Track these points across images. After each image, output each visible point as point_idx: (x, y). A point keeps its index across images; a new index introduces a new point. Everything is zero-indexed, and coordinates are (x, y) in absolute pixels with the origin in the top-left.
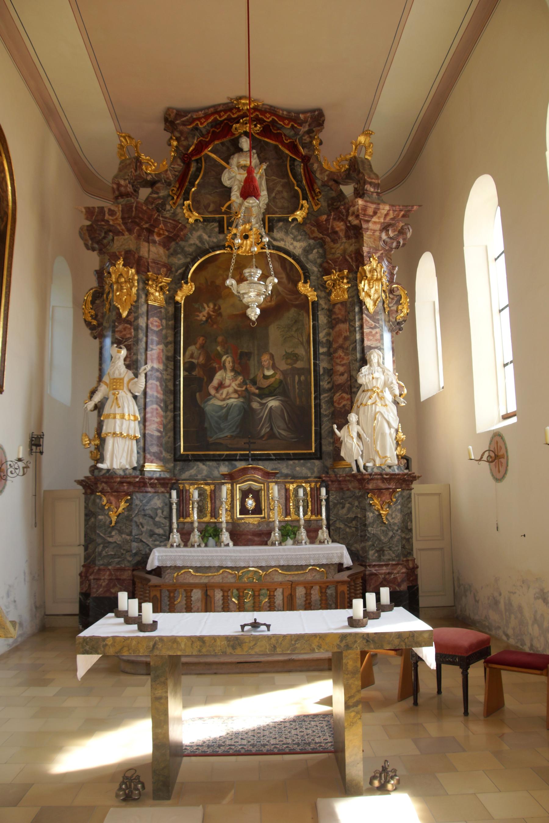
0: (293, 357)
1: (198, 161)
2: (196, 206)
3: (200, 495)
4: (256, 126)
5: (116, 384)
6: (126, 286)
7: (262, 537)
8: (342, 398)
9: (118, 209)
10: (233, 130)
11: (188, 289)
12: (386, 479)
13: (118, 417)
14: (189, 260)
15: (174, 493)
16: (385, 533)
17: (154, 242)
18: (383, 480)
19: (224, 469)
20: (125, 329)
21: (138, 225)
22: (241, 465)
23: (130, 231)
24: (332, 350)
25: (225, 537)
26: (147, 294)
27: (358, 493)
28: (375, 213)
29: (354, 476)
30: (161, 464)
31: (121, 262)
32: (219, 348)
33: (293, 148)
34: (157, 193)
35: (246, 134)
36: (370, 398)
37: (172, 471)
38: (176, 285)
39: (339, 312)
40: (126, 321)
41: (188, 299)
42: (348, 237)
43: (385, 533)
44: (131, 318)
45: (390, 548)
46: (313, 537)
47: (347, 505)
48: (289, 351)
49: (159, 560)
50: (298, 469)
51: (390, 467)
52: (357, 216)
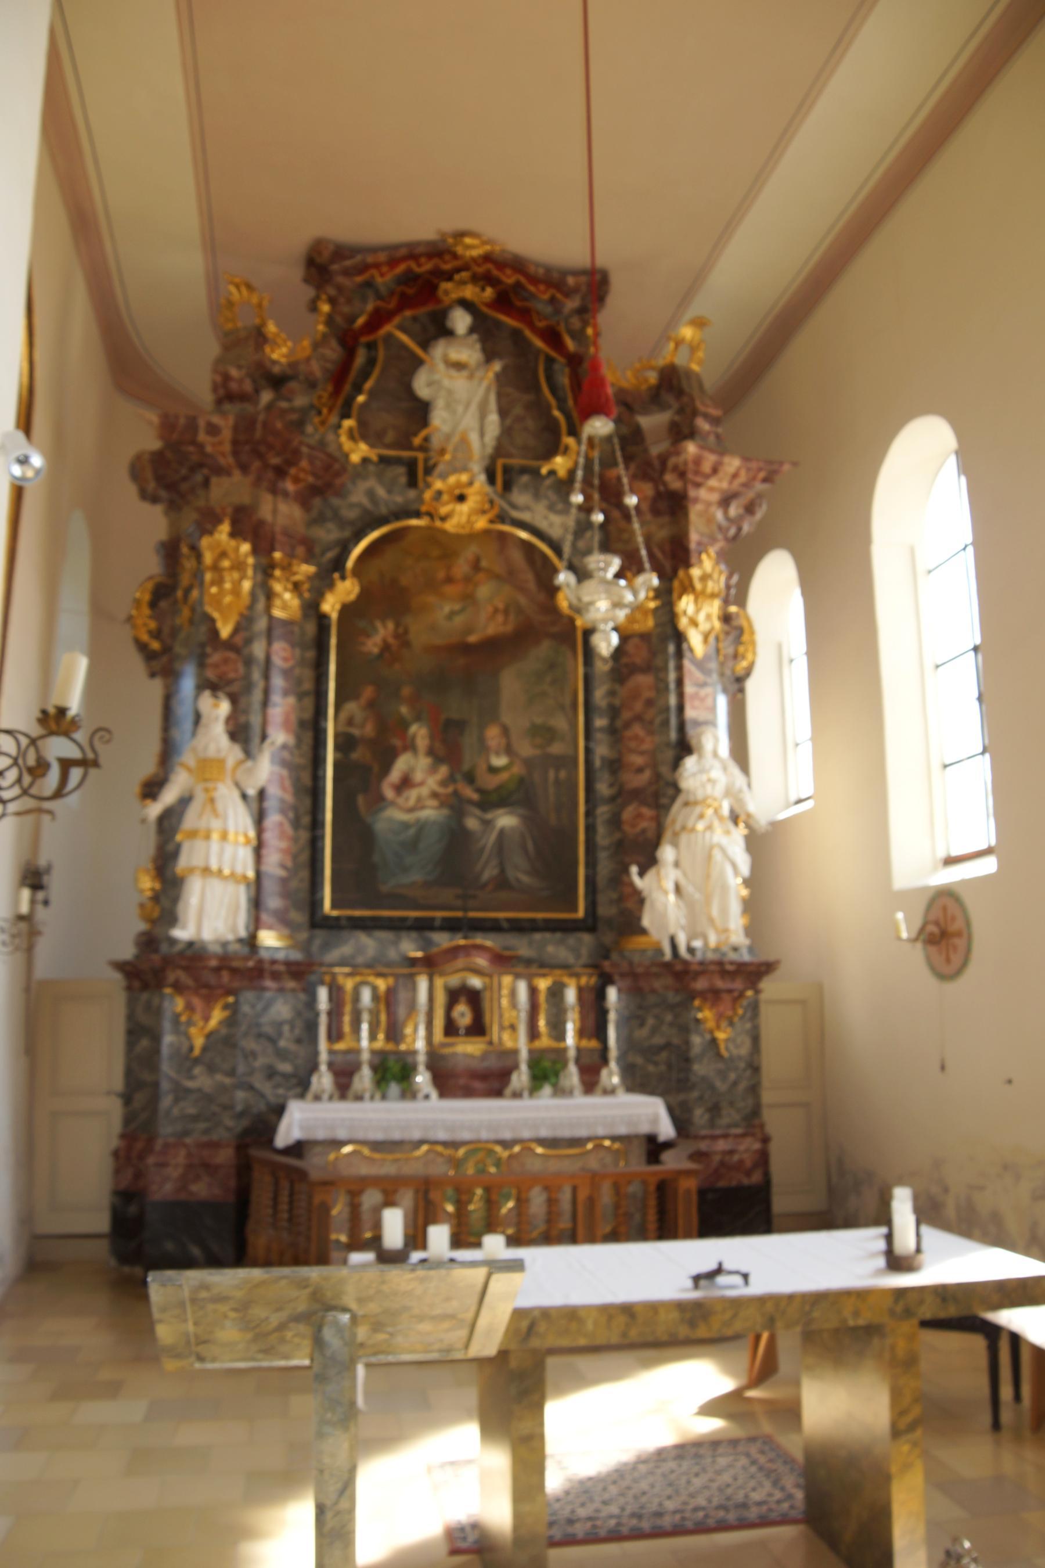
0: (544, 733)
1: (371, 346)
2: (363, 433)
3: (375, 997)
4: (483, 289)
7: (492, 1081)
8: (639, 816)
9: (226, 424)
10: (440, 293)
12: (728, 973)
13: (215, 836)
14: (347, 533)
15: (323, 994)
17: (286, 494)
20: (226, 661)
21: (260, 456)
22: (443, 940)
23: (244, 468)
24: (619, 723)
25: (422, 1079)
26: (270, 596)
27: (672, 998)
28: (715, 471)
29: (667, 966)
30: (286, 932)
31: (225, 528)
32: (404, 710)
33: (553, 337)
34: (289, 400)
36: (701, 816)
37: (306, 947)
38: (323, 582)
40: (229, 645)
41: (346, 610)
43: (723, 1074)
44: (238, 640)
45: (731, 1104)
47: (650, 1021)
48: (539, 721)
49: (302, 1128)
50: (550, 949)
51: (735, 949)
52: (682, 475)
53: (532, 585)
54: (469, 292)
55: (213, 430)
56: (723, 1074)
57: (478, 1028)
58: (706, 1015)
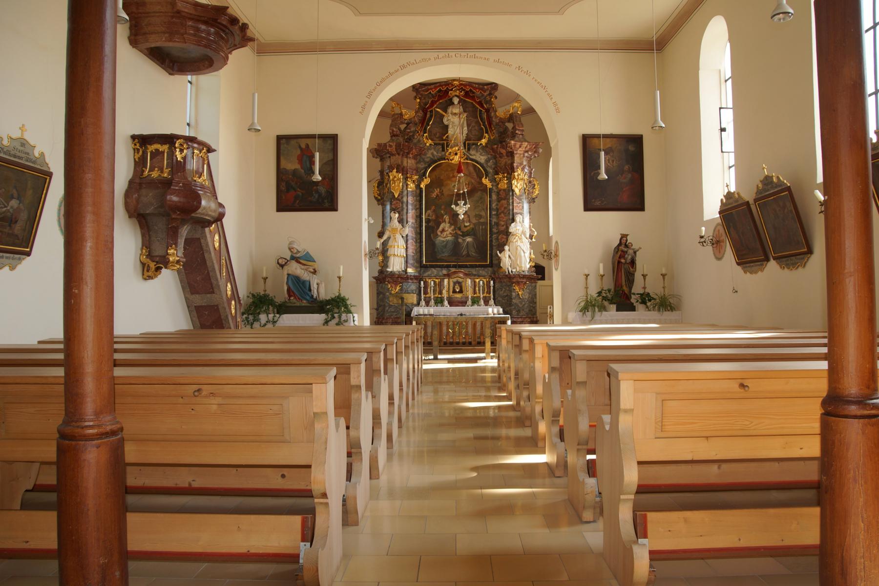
1: (431, 112)
5: (394, 230)
6: (396, 178)
7: (463, 303)
11: (427, 181)
16: (521, 303)
18: (520, 278)
19: (445, 272)
22: (453, 270)
23: (399, 154)
25: (446, 303)
26: (407, 185)
35: (457, 96)
37: (419, 272)
39: (503, 195)
40: (397, 199)
41: (427, 186)
42: (508, 156)
46: (487, 303)
53: (475, 177)
54: (457, 93)
55: (391, 146)
56: (521, 303)
57: (461, 291)
58: (517, 288)
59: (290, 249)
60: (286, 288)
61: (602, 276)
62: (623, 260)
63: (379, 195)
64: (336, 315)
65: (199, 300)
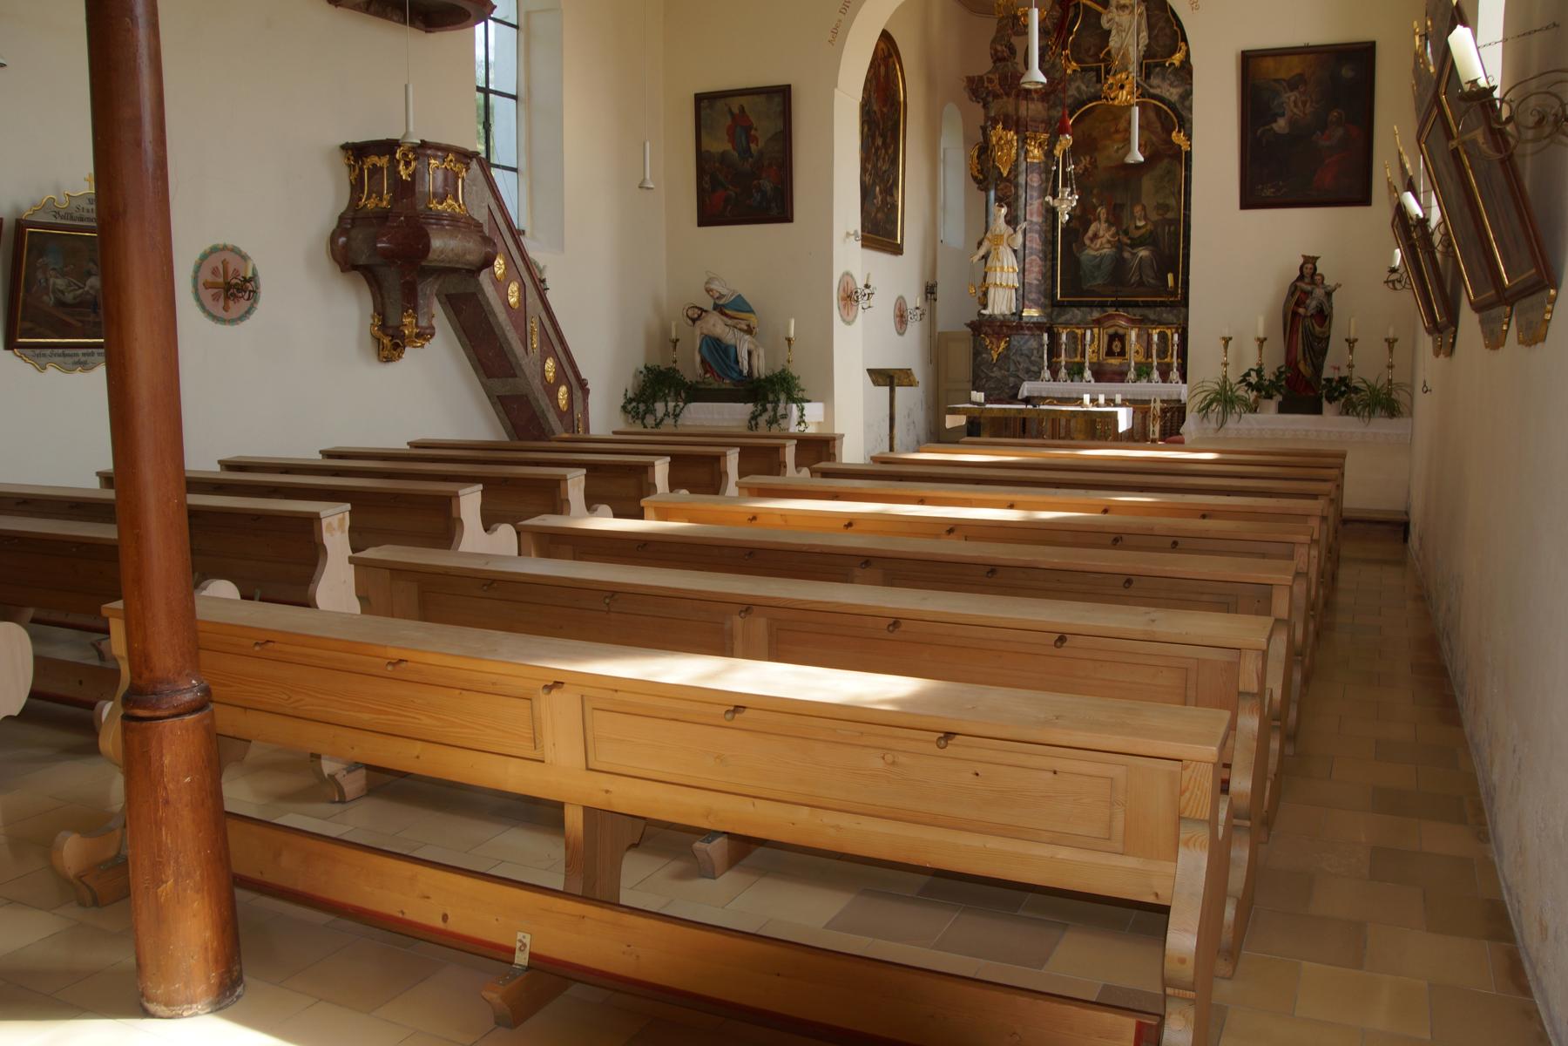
7: (1120, 376)
9: (995, 77)
11: (1067, 140)
15: (1046, 336)
19: (1096, 314)
22: (1111, 311)
23: (1008, 95)
25: (1088, 374)
26: (1027, 152)
37: (1049, 316)
40: (1007, 179)
55: (990, 81)
59: (708, 291)
60: (698, 359)
61: (1261, 341)
62: (1306, 309)
63: (981, 172)
64: (769, 406)
65: (501, 387)
